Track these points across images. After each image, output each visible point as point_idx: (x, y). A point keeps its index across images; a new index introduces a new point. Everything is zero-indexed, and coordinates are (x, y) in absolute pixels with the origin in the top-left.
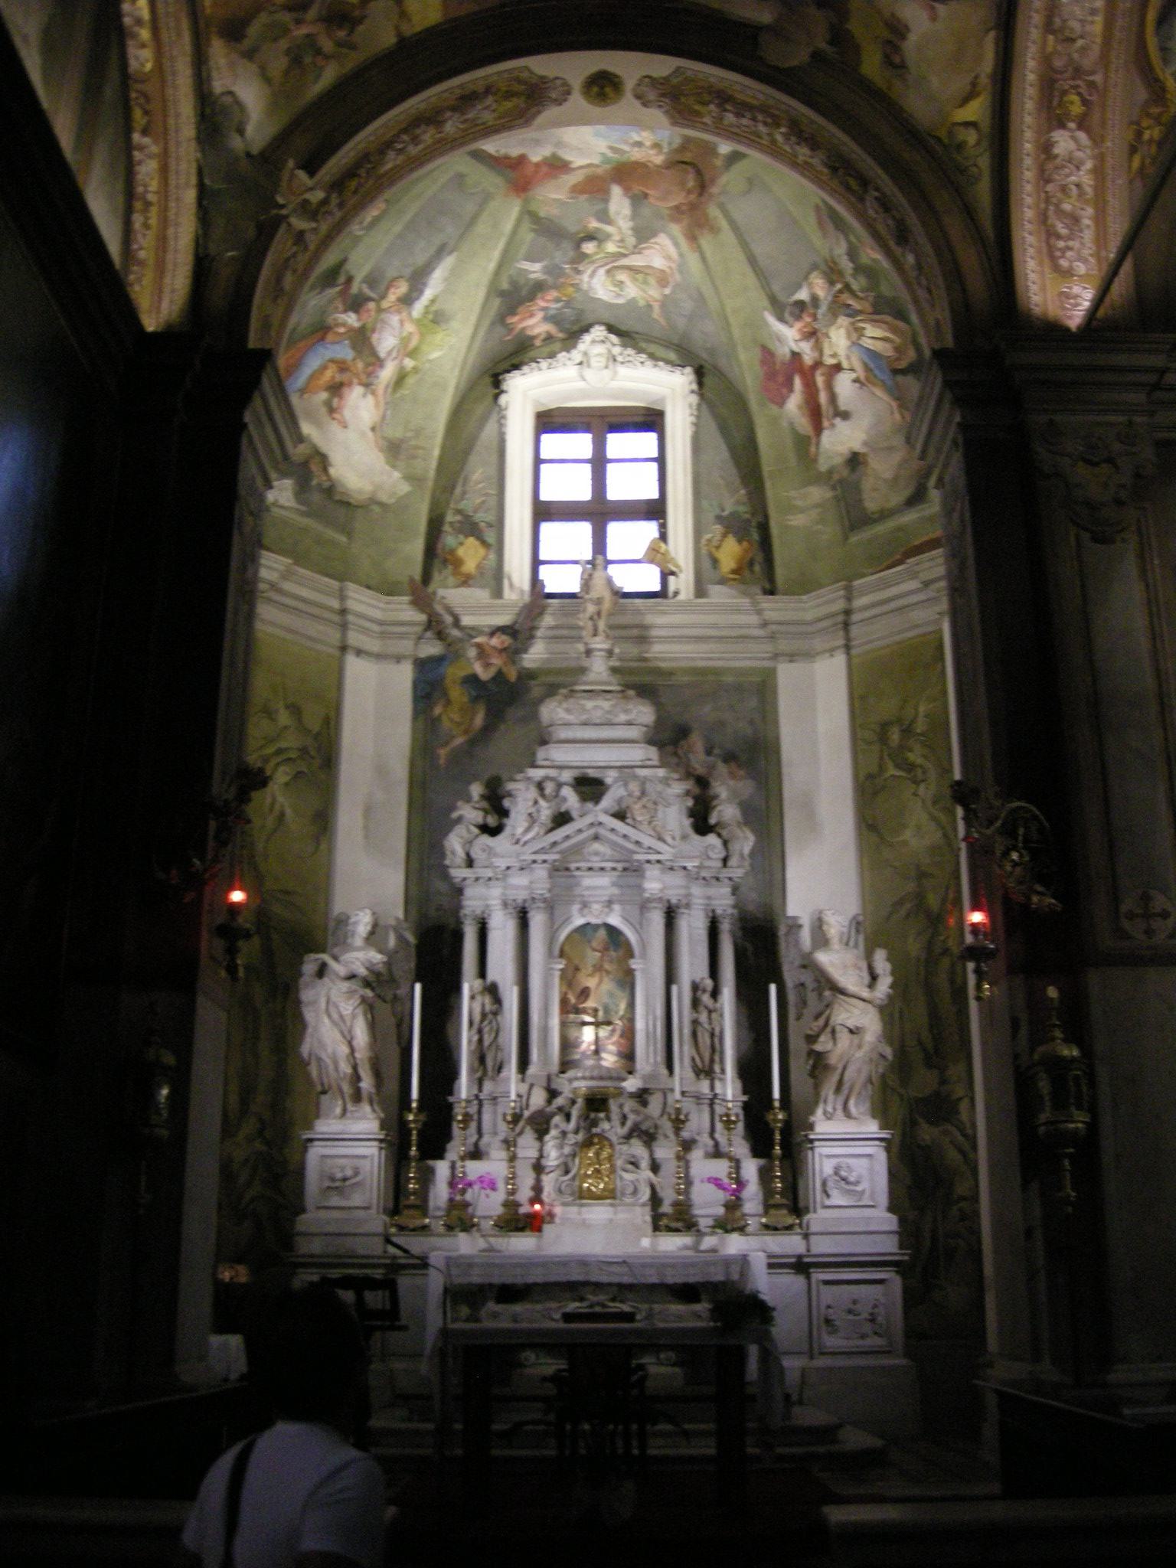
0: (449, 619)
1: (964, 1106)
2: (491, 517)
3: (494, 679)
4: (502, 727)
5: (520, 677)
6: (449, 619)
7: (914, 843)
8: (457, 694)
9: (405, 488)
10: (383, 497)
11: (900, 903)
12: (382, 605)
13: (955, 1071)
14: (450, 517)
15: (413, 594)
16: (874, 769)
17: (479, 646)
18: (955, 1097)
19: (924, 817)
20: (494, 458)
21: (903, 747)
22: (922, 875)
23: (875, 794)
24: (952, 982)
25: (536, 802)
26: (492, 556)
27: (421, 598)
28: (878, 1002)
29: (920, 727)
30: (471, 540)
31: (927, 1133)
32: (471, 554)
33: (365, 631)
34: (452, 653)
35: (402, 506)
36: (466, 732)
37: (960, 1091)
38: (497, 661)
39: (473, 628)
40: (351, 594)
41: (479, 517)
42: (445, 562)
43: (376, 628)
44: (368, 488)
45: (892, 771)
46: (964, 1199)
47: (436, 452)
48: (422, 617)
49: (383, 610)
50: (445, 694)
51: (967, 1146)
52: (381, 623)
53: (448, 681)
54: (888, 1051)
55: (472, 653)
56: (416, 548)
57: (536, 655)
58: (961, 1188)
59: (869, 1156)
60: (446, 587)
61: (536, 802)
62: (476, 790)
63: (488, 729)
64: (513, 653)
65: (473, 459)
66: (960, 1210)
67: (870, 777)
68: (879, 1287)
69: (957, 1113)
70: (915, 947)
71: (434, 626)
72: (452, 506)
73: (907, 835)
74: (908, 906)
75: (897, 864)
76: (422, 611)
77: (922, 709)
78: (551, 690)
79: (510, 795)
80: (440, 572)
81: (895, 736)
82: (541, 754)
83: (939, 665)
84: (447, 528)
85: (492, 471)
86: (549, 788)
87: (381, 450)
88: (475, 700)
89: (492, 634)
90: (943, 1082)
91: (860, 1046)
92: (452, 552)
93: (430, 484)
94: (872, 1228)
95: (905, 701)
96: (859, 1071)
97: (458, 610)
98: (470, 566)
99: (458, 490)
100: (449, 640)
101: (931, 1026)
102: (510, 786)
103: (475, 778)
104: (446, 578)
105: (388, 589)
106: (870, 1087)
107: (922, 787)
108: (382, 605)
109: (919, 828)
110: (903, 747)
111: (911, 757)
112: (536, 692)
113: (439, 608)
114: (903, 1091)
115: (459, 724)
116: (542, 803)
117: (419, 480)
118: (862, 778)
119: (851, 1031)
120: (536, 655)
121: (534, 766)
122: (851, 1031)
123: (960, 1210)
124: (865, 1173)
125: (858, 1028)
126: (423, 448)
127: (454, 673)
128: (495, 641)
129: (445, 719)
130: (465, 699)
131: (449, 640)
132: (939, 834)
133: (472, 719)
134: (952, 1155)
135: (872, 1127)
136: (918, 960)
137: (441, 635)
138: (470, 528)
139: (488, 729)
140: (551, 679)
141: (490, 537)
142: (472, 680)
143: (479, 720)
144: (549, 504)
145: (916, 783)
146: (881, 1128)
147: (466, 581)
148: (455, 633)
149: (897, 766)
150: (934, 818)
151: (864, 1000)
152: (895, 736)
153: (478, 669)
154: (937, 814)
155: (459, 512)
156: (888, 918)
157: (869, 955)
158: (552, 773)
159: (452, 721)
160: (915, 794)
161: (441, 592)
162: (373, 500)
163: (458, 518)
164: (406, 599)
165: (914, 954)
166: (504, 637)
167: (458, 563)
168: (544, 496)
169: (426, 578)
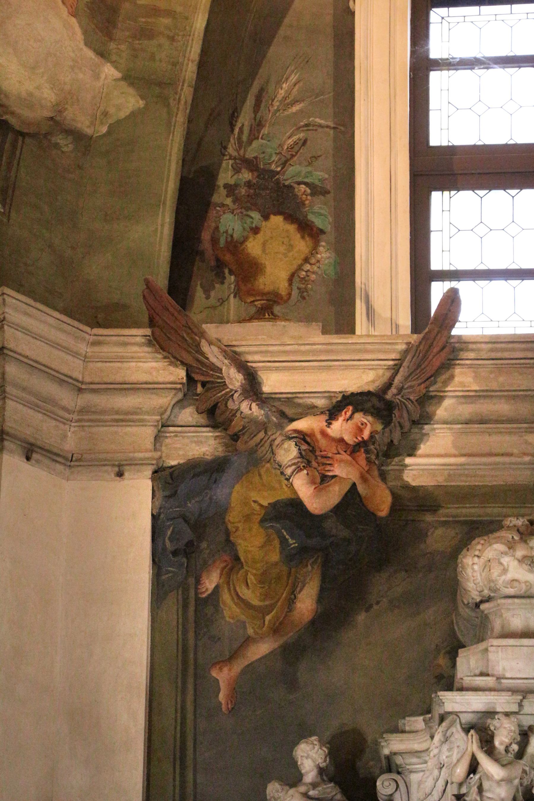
0: (235, 379)
2: (319, 175)
3: (338, 509)
4: (361, 618)
5: (393, 509)
6: (235, 379)
8: (254, 544)
9: (129, 102)
10: (83, 123)
12: (83, 348)
14: (226, 176)
15: (152, 323)
17: (303, 437)
20: (325, 50)
25: (474, 767)
26: (325, 255)
27: (172, 336)
30: (277, 220)
32: (276, 250)
33: (43, 405)
34: (243, 449)
35: (122, 139)
36: (276, 630)
38: (345, 471)
39: (290, 400)
40: (12, 316)
41: (294, 172)
42: (219, 268)
43: (66, 397)
44: (49, 95)
47: (200, 23)
48: (181, 373)
49: (86, 359)
50: (229, 544)
52: (79, 387)
53: (233, 517)
55: (288, 453)
56: (157, 232)
57: (434, 458)
60: (223, 321)
61: (474, 767)
62: (310, 757)
63: (330, 620)
64: (384, 453)
65: (276, 52)
71: (202, 390)
72: (231, 150)
76: (175, 360)
78: (478, 529)
79: (390, 766)
80: (207, 292)
82: (467, 664)
84: (220, 196)
85: (322, 77)
86: (504, 735)
87: (74, 14)
88: (295, 558)
89: (333, 413)
92: (235, 246)
93: (186, 93)
97: (254, 359)
98: (275, 275)
99: (245, 119)
100: (237, 425)
102: (393, 744)
103: (304, 733)
104: (222, 301)
105: (98, 313)
108: (83, 348)
112: (438, 539)
113: (213, 354)
115: (263, 611)
116: (487, 764)
117: (160, 84)
120: (434, 458)
121: (450, 687)
126: (170, 13)
127: (245, 498)
128: (340, 428)
129: (226, 596)
130: (275, 557)
131: (237, 425)
133: (291, 601)
137: (215, 416)
138: (275, 197)
139: (330, 620)
140: (470, 511)
141: (320, 214)
142: (289, 512)
143: (306, 603)
144: (450, 152)
147: (267, 308)
148: (250, 409)
153: (302, 487)
155: (251, 164)
158: (503, 702)
159: (245, 604)
161: (212, 330)
162: (56, 124)
163: (246, 175)
164: (139, 334)
166: (359, 417)
167: (248, 271)
168: (437, 138)
169: (180, 288)
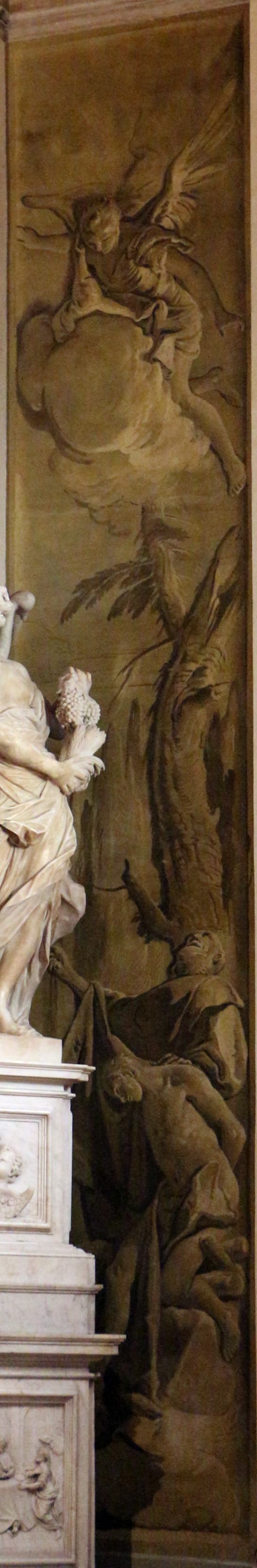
1: (224, 1028)
7: (140, 459)
11: (102, 581)
13: (210, 948)
16: (53, 292)
18: (206, 1002)
19: (171, 408)
21: (128, 252)
22: (154, 529)
23: (55, 346)
24: (212, 761)
28: (74, 785)
29: (173, 213)
31: (135, 1076)
37: (215, 991)
45: (96, 301)
46: (218, 1224)
51: (227, 1115)
54: (78, 895)
58: (213, 1198)
59: (46, 1116)
66: (204, 1246)
67: (38, 309)
68: (51, 1415)
69: (207, 1036)
70: (135, 684)
73: (126, 441)
74: (117, 592)
75: (95, 501)
77: (178, 178)
81: (109, 229)
83: (230, 89)
90: (178, 968)
91: (28, 877)
94: (41, 1280)
95: (138, 158)
96: (24, 929)
101: (157, 855)
106: (37, 966)
107: (168, 342)
109: (155, 428)
110: (128, 252)
111: (146, 277)
114: (81, 982)
118: (20, 313)
119: (14, 840)
122: (14, 840)
123: (204, 1246)
124: (30, 1155)
125: (27, 835)
132: (203, 447)
134: (192, 1129)
135: (47, 1054)
136: (135, 706)
145: (158, 335)
146: (67, 1058)
149: (108, 294)
150: (187, 411)
151: (44, 776)
152: (109, 229)
154: (196, 402)
156: (66, 616)
157: (47, 680)
160: (150, 357)
165: (125, 694)
